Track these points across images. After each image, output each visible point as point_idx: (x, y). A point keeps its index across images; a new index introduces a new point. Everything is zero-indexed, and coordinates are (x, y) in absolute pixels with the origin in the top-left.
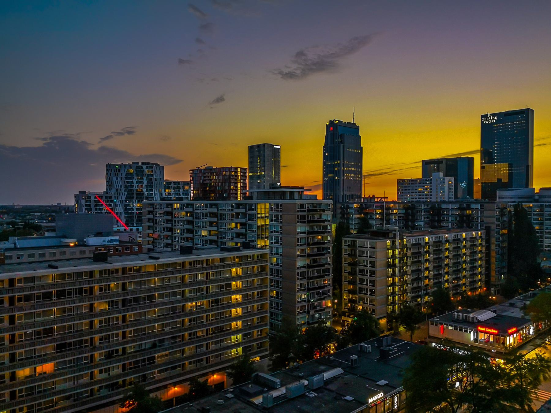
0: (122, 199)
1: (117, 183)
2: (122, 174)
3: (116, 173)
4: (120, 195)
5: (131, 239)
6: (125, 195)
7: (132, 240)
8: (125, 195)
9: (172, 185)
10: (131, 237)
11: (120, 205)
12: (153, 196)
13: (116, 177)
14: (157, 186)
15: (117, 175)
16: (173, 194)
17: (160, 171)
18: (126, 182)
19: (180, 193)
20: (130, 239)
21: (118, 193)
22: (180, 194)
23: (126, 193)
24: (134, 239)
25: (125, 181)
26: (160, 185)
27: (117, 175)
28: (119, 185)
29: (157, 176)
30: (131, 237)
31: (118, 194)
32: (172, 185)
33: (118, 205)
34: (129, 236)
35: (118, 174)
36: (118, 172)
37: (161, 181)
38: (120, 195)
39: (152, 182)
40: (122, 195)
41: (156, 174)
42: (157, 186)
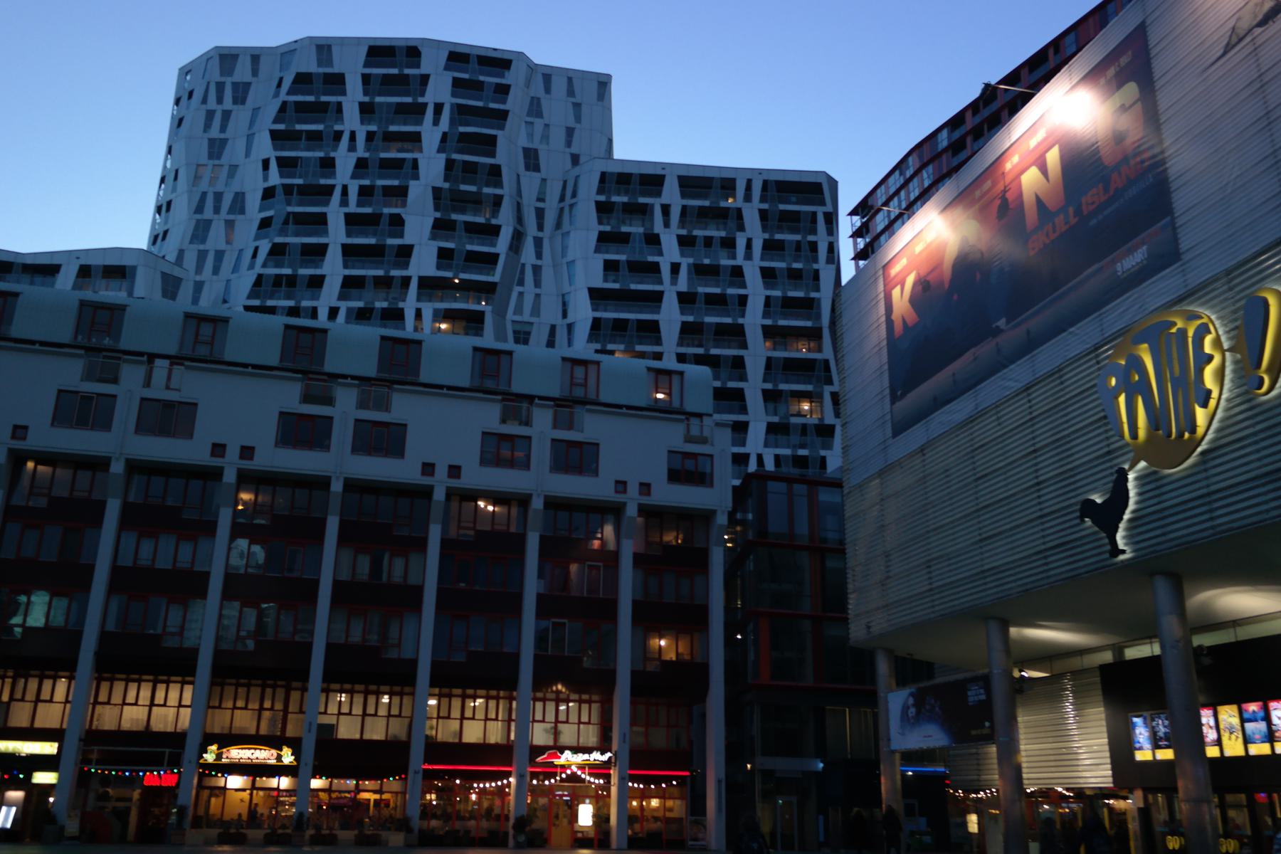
2: (256, 110)
3: (210, 115)
4: (216, 271)
6: (251, 267)
8: (251, 267)
9: (671, 194)
12: (496, 278)
13: (212, 142)
14: (540, 213)
15: (223, 128)
16: (675, 268)
17: (577, 106)
18: (273, 164)
19: (740, 260)
21: (202, 256)
22: (737, 272)
23: (265, 247)
25: (266, 164)
26: (568, 200)
27: (223, 128)
28: (218, 197)
29: (545, 138)
31: (199, 268)
32: (671, 194)
35: (227, 115)
36: (228, 103)
37: (576, 171)
38: (216, 271)
39: (495, 172)
40: (236, 269)
42: (540, 213)
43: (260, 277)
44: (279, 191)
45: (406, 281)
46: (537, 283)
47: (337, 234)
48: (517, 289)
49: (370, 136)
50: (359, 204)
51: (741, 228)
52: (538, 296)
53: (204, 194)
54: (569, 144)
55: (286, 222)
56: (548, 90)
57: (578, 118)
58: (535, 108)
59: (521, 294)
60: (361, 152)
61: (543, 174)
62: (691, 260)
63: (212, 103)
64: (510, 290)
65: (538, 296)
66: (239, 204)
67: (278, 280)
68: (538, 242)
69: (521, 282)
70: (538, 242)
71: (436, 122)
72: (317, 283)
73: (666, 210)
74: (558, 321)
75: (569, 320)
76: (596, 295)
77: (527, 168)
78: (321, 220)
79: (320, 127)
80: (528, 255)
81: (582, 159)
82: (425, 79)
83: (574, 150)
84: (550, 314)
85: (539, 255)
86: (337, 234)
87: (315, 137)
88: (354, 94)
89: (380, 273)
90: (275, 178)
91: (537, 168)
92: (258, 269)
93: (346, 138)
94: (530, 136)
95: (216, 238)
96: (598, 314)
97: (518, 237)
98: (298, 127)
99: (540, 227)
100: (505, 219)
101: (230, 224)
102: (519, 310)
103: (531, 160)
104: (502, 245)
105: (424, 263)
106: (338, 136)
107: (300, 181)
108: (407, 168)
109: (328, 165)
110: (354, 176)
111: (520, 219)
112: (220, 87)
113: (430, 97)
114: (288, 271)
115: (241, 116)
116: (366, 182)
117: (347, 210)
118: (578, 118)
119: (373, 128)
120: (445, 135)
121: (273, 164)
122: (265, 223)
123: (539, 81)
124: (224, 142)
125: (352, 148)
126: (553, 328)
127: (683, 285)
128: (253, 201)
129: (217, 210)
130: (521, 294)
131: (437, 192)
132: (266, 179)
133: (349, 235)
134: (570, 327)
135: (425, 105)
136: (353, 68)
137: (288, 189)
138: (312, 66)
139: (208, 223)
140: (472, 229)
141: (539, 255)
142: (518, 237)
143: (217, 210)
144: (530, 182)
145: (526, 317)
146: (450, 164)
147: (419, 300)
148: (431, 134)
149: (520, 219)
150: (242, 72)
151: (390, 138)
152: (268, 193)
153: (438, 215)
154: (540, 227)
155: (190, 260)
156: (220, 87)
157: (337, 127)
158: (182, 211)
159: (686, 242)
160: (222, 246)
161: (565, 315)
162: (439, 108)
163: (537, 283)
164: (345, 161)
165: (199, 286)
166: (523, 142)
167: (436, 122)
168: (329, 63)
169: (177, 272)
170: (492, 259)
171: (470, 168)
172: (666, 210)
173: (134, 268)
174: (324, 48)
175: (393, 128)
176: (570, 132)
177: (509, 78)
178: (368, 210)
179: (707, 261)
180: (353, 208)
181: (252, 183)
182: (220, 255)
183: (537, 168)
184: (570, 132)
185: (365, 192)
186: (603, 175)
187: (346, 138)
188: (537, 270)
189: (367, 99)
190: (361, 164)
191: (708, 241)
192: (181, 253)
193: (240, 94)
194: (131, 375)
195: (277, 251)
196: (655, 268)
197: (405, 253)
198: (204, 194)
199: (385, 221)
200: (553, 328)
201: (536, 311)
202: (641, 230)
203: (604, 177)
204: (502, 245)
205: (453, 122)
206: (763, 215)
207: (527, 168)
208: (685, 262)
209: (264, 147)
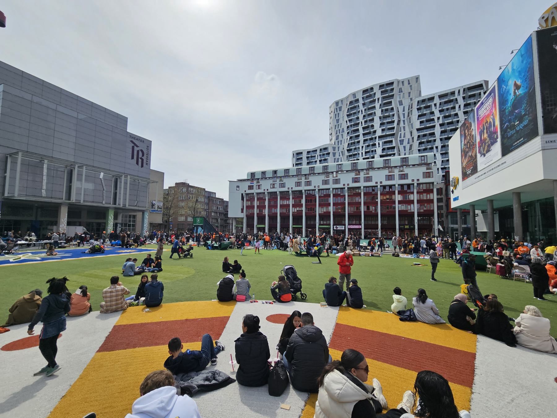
0: (343, 149)
1: (338, 128)
3: (336, 115)
5: (136, 149)
6: (347, 142)
7: (138, 152)
8: (347, 142)
9: (437, 101)
10: (137, 146)
11: (342, 158)
14: (404, 114)
15: (338, 117)
16: (438, 118)
18: (348, 121)
20: (133, 148)
21: (338, 142)
22: (456, 115)
23: (349, 138)
24: (142, 151)
25: (347, 121)
26: (410, 110)
27: (338, 117)
28: (339, 130)
29: (403, 97)
30: (137, 146)
33: (339, 158)
34: (132, 141)
35: (338, 114)
36: (338, 112)
41: (402, 94)
42: (404, 114)
43: (349, 143)
44: (350, 126)
45: (376, 138)
46: (404, 130)
47: (361, 132)
48: (400, 133)
49: (365, 110)
50: (365, 125)
51: (457, 103)
52: (405, 133)
53: (337, 130)
54: (409, 96)
55: (352, 132)
56: (403, 85)
57: (411, 89)
58: (401, 91)
59: (401, 134)
60: (364, 114)
61: (404, 105)
62: (443, 115)
63: (336, 112)
64: (398, 133)
65: (405, 133)
66: (343, 131)
67: (352, 144)
68: (404, 121)
69: (401, 131)
70: (404, 121)
71: (378, 102)
72: (359, 142)
73: (435, 105)
74: (410, 137)
75: (413, 136)
76: (418, 130)
77: (400, 105)
78: (358, 130)
79: (356, 111)
80: (402, 124)
81: (413, 99)
82: (375, 94)
83: (411, 97)
84: (408, 136)
85: (404, 124)
86: (361, 132)
87: (355, 113)
88: (361, 102)
89: (370, 137)
90: (349, 124)
91: (402, 104)
92: (348, 142)
93: (360, 112)
94: (400, 98)
95: (340, 138)
96: (419, 134)
97: (399, 121)
98: (351, 112)
99: (404, 117)
100: (396, 119)
101: (342, 135)
102: (400, 137)
103: (401, 103)
104: (395, 125)
105: (379, 133)
106: (359, 112)
107: (353, 123)
108: (373, 114)
109: (358, 118)
110: (363, 119)
111: (399, 117)
112: (337, 109)
113: (376, 98)
114: (353, 141)
115: (341, 113)
116: (365, 120)
117: (362, 126)
118: (411, 89)
119: (366, 108)
120: (380, 104)
121: (348, 121)
122: (348, 133)
123: (401, 83)
124: (339, 119)
125: (362, 113)
126: (409, 139)
127: (441, 121)
128: (345, 129)
129: (340, 133)
130: (401, 134)
131: (380, 118)
132: (347, 124)
133: (364, 131)
134: (413, 138)
135: (375, 99)
136: (360, 96)
137: (351, 126)
138: (353, 99)
139: (338, 136)
140: (388, 123)
141: (404, 124)
142: (399, 121)
143: (340, 133)
144: (401, 108)
145: (402, 138)
146: (382, 111)
147: (379, 141)
148: (377, 105)
149: (399, 117)
150: (340, 105)
151: (369, 109)
152: (348, 127)
153: (381, 122)
154: (404, 117)
155: (337, 143)
156: (337, 109)
157: (359, 110)
158: (334, 134)
159: (440, 111)
160: (341, 139)
161: (411, 135)
162: (378, 99)
163: (404, 130)
164: (361, 116)
165: (339, 148)
166: (398, 99)
167: (378, 102)
168: (355, 97)
169: (335, 146)
170: (393, 128)
171: (387, 110)
172: (435, 105)
173: (328, 147)
174: (354, 95)
175: (369, 107)
176: (409, 93)
177: (395, 86)
178: (367, 125)
179: (447, 114)
180: (364, 126)
181: (345, 126)
182: (341, 141)
183: (402, 104)
184: (409, 93)
185: (366, 122)
186: (418, 101)
187: (360, 112)
188: (404, 128)
189: (364, 102)
190: (364, 116)
191: (448, 109)
192: (335, 142)
193: (340, 109)
194: (331, 176)
195: (351, 138)
196: (433, 120)
197: (375, 132)
198: (337, 130)
199: (370, 126)
200: (409, 139)
201: (404, 137)
202: (429, 111)
203: (418, 102)
204: (395, 125)
205: (382, 101)
206: (464, 98)
207: (400, 105)
208: (441, 116)
209: (346, 119)
